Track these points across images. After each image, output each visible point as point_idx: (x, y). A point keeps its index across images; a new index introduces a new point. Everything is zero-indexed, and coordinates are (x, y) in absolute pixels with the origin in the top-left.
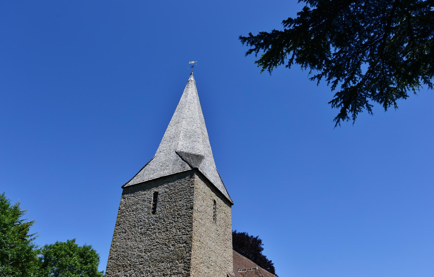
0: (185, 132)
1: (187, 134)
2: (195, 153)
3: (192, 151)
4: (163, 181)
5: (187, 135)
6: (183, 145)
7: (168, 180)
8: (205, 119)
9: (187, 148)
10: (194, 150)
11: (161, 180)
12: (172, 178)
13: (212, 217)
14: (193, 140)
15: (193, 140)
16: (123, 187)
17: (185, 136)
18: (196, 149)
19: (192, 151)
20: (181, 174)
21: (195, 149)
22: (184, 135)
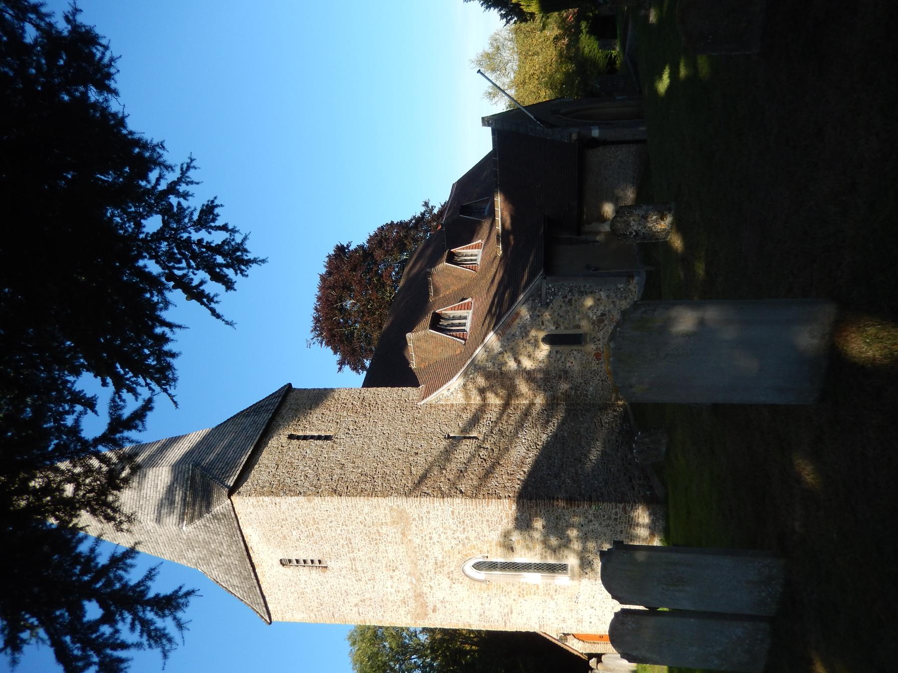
1: (138, 503)
5: (141, 503)
15: (152, 491)
17: (143, 509)
20: (240, 521)
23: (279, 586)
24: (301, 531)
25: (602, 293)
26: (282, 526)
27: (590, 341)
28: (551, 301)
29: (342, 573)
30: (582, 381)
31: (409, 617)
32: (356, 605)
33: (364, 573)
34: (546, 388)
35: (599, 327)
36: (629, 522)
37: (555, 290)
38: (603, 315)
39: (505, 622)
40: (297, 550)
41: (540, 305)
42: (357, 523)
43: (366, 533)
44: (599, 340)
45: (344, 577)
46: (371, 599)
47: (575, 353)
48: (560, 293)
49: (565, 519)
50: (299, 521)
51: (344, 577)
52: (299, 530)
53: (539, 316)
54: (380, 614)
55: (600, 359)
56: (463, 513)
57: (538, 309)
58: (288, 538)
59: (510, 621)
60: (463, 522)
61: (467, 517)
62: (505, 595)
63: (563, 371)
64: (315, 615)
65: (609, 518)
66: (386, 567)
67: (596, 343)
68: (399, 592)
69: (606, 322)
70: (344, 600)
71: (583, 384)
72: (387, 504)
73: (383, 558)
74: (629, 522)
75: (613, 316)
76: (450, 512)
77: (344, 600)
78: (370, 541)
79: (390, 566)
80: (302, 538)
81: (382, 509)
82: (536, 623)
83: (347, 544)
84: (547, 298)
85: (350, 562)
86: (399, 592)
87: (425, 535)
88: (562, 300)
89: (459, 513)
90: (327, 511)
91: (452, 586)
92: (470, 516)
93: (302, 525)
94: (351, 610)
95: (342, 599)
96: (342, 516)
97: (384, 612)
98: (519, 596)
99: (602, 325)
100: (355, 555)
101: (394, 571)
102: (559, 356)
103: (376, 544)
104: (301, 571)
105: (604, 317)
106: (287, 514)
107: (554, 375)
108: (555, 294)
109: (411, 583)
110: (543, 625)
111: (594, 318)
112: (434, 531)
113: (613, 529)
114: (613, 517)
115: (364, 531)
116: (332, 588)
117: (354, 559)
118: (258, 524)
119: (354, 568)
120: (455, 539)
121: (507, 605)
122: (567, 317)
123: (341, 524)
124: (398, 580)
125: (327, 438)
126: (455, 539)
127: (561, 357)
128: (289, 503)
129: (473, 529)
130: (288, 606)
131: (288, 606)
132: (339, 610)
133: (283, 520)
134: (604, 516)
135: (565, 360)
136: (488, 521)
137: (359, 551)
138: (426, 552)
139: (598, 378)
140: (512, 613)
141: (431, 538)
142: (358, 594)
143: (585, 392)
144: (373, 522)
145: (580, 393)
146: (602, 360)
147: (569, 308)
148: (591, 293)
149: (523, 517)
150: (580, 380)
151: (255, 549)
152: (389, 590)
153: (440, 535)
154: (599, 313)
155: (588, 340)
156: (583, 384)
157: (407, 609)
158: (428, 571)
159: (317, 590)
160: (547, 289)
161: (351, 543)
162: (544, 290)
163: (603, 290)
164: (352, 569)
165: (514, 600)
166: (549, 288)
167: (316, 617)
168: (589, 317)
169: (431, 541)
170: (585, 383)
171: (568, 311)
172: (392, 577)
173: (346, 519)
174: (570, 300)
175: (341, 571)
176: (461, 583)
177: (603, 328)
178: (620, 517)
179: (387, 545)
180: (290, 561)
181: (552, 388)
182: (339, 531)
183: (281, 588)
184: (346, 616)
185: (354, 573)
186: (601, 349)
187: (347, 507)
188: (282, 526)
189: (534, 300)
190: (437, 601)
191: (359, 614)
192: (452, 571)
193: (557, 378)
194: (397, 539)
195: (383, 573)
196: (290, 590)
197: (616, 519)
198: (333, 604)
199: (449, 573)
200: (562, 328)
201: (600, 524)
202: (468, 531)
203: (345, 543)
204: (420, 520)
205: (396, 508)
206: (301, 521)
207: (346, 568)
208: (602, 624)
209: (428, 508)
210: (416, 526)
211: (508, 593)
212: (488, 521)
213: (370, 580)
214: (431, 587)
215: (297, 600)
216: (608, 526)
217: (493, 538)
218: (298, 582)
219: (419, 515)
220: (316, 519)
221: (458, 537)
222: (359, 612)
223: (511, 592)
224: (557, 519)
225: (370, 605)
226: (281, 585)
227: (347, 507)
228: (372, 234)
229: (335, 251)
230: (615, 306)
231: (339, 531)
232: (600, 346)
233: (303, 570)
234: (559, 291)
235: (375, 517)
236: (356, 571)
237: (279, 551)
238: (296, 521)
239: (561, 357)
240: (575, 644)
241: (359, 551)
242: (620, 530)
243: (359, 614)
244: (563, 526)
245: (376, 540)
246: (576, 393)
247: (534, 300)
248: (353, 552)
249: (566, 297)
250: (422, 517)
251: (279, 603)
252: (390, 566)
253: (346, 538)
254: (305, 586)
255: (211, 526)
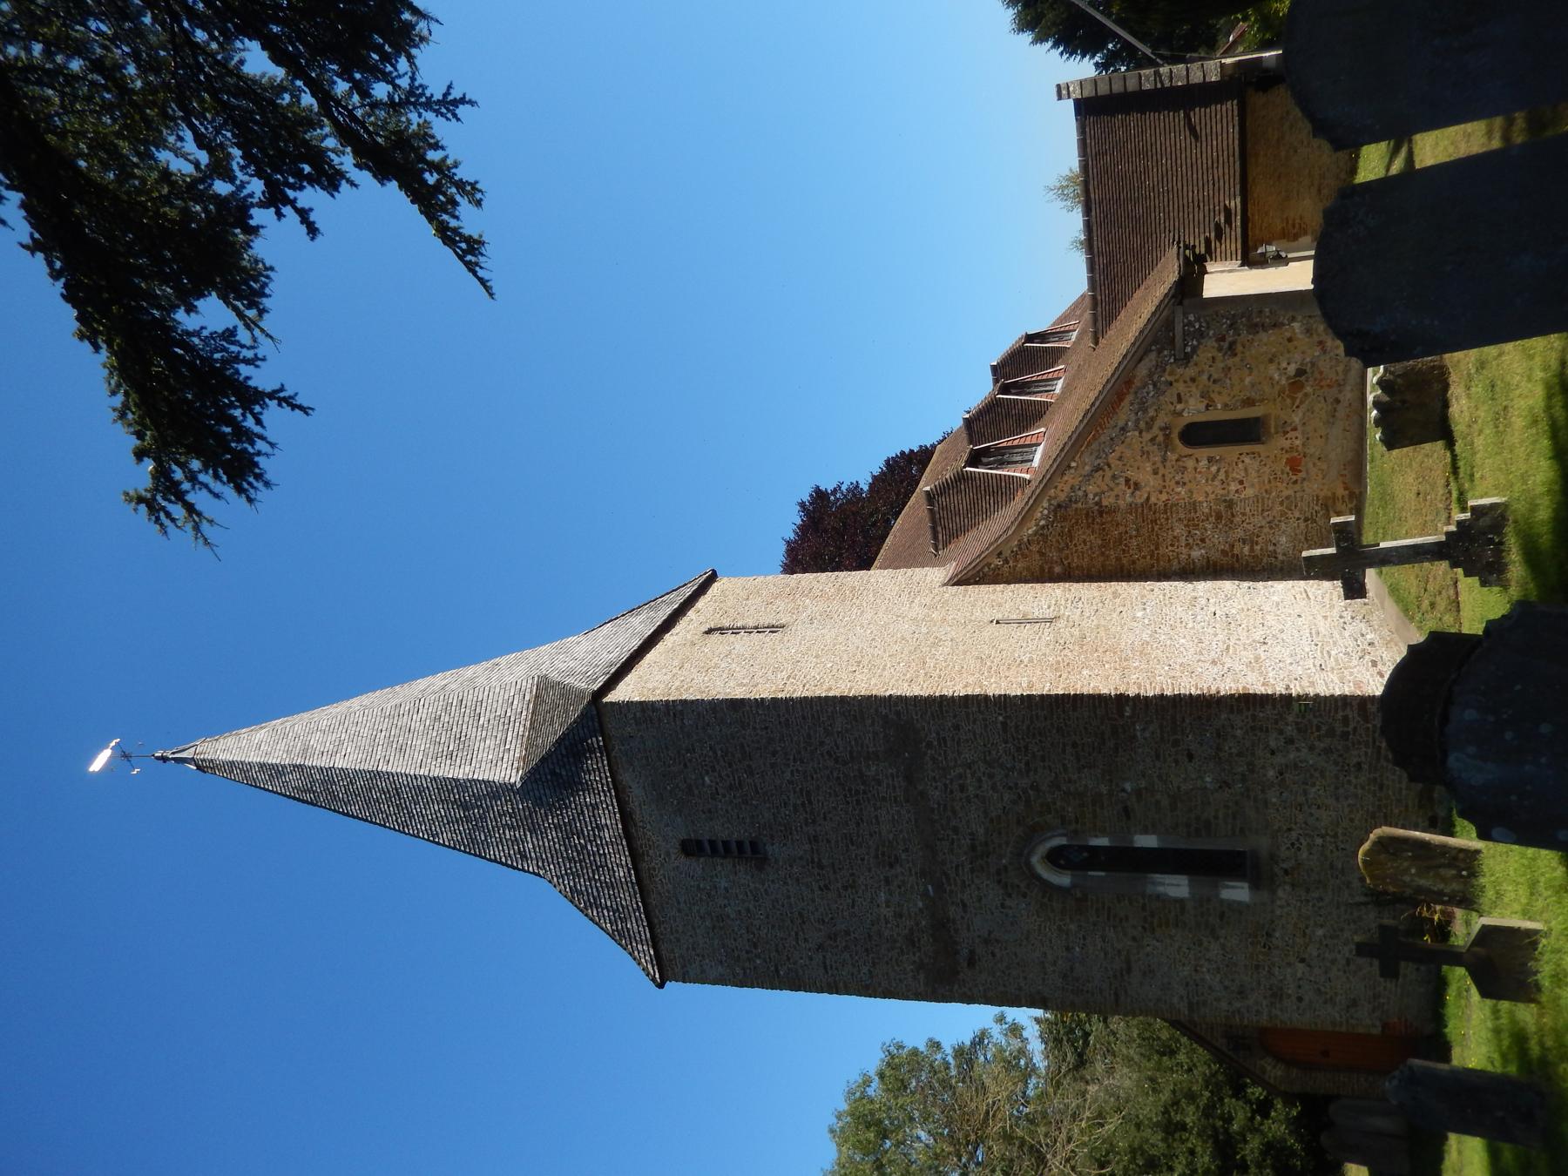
0: (439, 760)
1: (446, 749)
2: (524, 713)
3: (517, 724)
4: (641, 824)
5: (451, 749)
6: (494, 762)
7: (636, 804)
8: (374, 690)
9: (507, 747)
10: (512, 719)
11: (636, 831)
12: (628, 790)
13: (768, 639)
14: (470, 727)
15: (470, 727)
16: (661, 986)
17: (454, 758)
18: (509, 710)
19: (517, 724)
20: (613, 754)
21: (508, 714)
22: (448, 762)
23: (679, 903)
24: (720, 776)
25: (1296, 325)
26: (685, 765)
27: (1277, 433)
28: (1194, 349)
29: (795, 869)
30: (1263, 523)
31: (922, 977)
32: (820, 947)
33: (835, 872)
34: (1191, 541)
35: (1294, 399)
36: (1374, 742)
37: (1201, 326)
38: (1300, 372)
39: (1116, 994)
40: (711, 819)
41: (1172, 360)
42: (822, 755)
43: (838, 778)
44: (1295, 429)
45: (798, 880)
46: (847, 933)
47: (1247, 460)
48: (1211, 333)
49: (1234, 737)
50: (715, 753)
51: (798, 880)
52: (716, 774)
53: (1171, 384)
54: (865, 970)
55: (1300, 471)
56: (1024, 728)
57: (1168, 367)
58: (696, 792)
59: (1126, 992)
60: (1026, 748)
61: (1034, 735)
62: (1114, 927)
63: (1225, 501)
64: (744, 969)
65: (1331, 733)
66: (876, 857)
67: (1288, 436)
68: (901, 916)
69: (1308, 389)
70: (797, 934)
71: (1266, 530)
72: (877, 710)
73: (871, 835)
74: (1374, 742)
75: (1321, 373)
76: (999, 725)
77: (797, 934)
78: (845, 796)
79: (883, 854)
80: (720, 791)
81: (869, 722)
82: (1182, 997)
83: (803, 804)
84: (1186, 345)
85: (807, 847)
86: (901, 916)
87: (952, 780)
88: (1216, 345)
89: (1017, 727)
90: (766, 728)
91: (1008, 903)
92: (1040, 734)
93: (722, 763)
94: (811, 959)
95: (793, 933)
96: (795, 739)
97: (874, 964)
98: (1143, 927)
99: (1300, 395)
100: (818, 829)
101: (891, 866)
102: (1214, 469)
103: (858, 801)
104: (719, 868)
105: (1303, 379)
106: (695, 737)
107: (1207, 510)
108: (1201, 335)
109: (925, 894)
110: (1198, 1003)
111: (1284, 382)
112: (968, 771)
113: (1340, 760)
114: (1339, 728)
115: (835, 775)
116: (774, 906)
117: (816, 839)
118: (644, 761)
119: (816, 860)
120: (1010, 788)
121: (1119, 951)
122: (1228, 381)
123: (792, 758)
124: (899, 887)
125: (773, 629)
126: (1010, 788)
127: (1218, 470)
128: (699, 714)
129: (1046, 764)
130: (694, 949)
131: (694, 949)
132: (789, 959)
133: (688, 751)
134: (1318, 728)
135: (1227, 477)
136: (1074, 745)
137: (825, 819)
138: (953, 823)
139: (1297, 514)
140: (1129, 970)
141: (962, 788)
142: (824, 921)
143: (1271, 548)
144: (851, 753)
145: (1261, 549)
146: (1303, 475)
147: (1230, 362)
148: (1275, 325)
149: (1147, 734)
150: (1259, 521)
151: (637, 817)
152: (884, 911)
153: (980, 780)
154: (1292, 369)
155: (1273, 430)
156: (1266, 530)
157: (916, 959)
158: (957, 866)
159: (748, 910)
160: (1184, 326)
161: (810, 803)
162: (1179, 328)
163: (1300, 318)
164: (813, 862)
165: (1134, 939)
166: (1190, 324)
167: (745, 973)
168: (1271, 378)
169: (965, 795)
170: (1271, 528)
171: (1230, 369)
172: (887, 881)
173: (802, 745)
174: (1232, 345)
175: (791, 866)
176: (1025, 896)
177: (1302, 402)
178: (1355, 729)
179: (878, 804)
180: (699, 843)
181: (1203, 540)
182: (788, 775)
183: (682, 905)
184: (801, 973)
185: (816, 871)
186: (1300, 449)
187: (804, 718)
188: (685, 765)
189: (1159, 352)
190: (977, 941)
191: (825, 968)
192: (1006, 867)
193: (1212, 519)
194: (898, 789)
195: (870, 870)
196: (698, 911)
197: (1345, 735)
198: (777, 945)
199: (998, 873)
200: (1219, 406)
201: (1311, 748)
202: (1036, 771)
203: (799, 802)
204: (940, 746)
205: (895, 717)
206: (719, 753)
207: (801, 858)
208: (1325, 1003)
209: (955, 716)
210: (933, 758)
211: (1121, 920)
212: (1074, 745)
213: (845, 888)
214: (964, 905)
215: (711, 935)
216: (1328, 751)
217: (1086, 786)
218: (713, 893)
219: (938, 734)
220: (747, 749)
221: (1016, 784)
222: (824, 963)
223: (1127, 918)
224: (1219, 735)
225: (846, 947)
226: (682, 900)
227: (804, 718)
228: (876, 472)
229: (811, 495)
230: (1324, 351)
231: (788, 775)
232: (1298, 442)
233: (722, 864)
234: (1208, 328)
235: (856, 739)
236: (821, 867)
237: (679, 820)
238: (711, 753)
239: (1218, 470)
240: (1269, 1068)
241: (825, 819)
242: (1355, 760)
243: (825, 968)
244: (1231, 754)
245: (857, 792)
246: (1252, 550)
247: (1159, 352)
248: (814, 822)
249: (1223, 339)
250: (944, 738)
251: (678, 940)
252: (883, 854)
253: (801, 790)
254: (726, 902)
255: (564, 773)
